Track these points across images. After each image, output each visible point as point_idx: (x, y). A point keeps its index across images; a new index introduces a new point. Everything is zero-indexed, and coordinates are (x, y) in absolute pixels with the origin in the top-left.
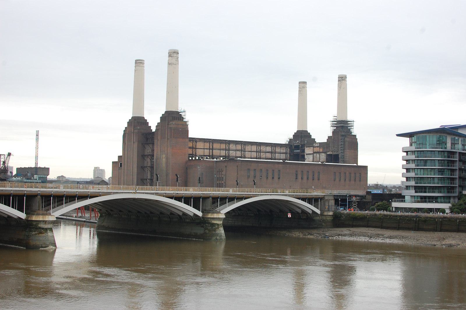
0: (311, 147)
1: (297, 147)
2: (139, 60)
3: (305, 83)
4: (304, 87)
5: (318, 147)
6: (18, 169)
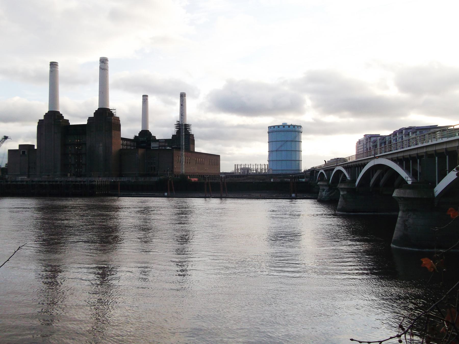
0: (158, 142)
1: (143, 142)
2: (55, 62)
3: (147, 96)
4: (147, 99)
5: (163, 142)
6: (328, 161)
